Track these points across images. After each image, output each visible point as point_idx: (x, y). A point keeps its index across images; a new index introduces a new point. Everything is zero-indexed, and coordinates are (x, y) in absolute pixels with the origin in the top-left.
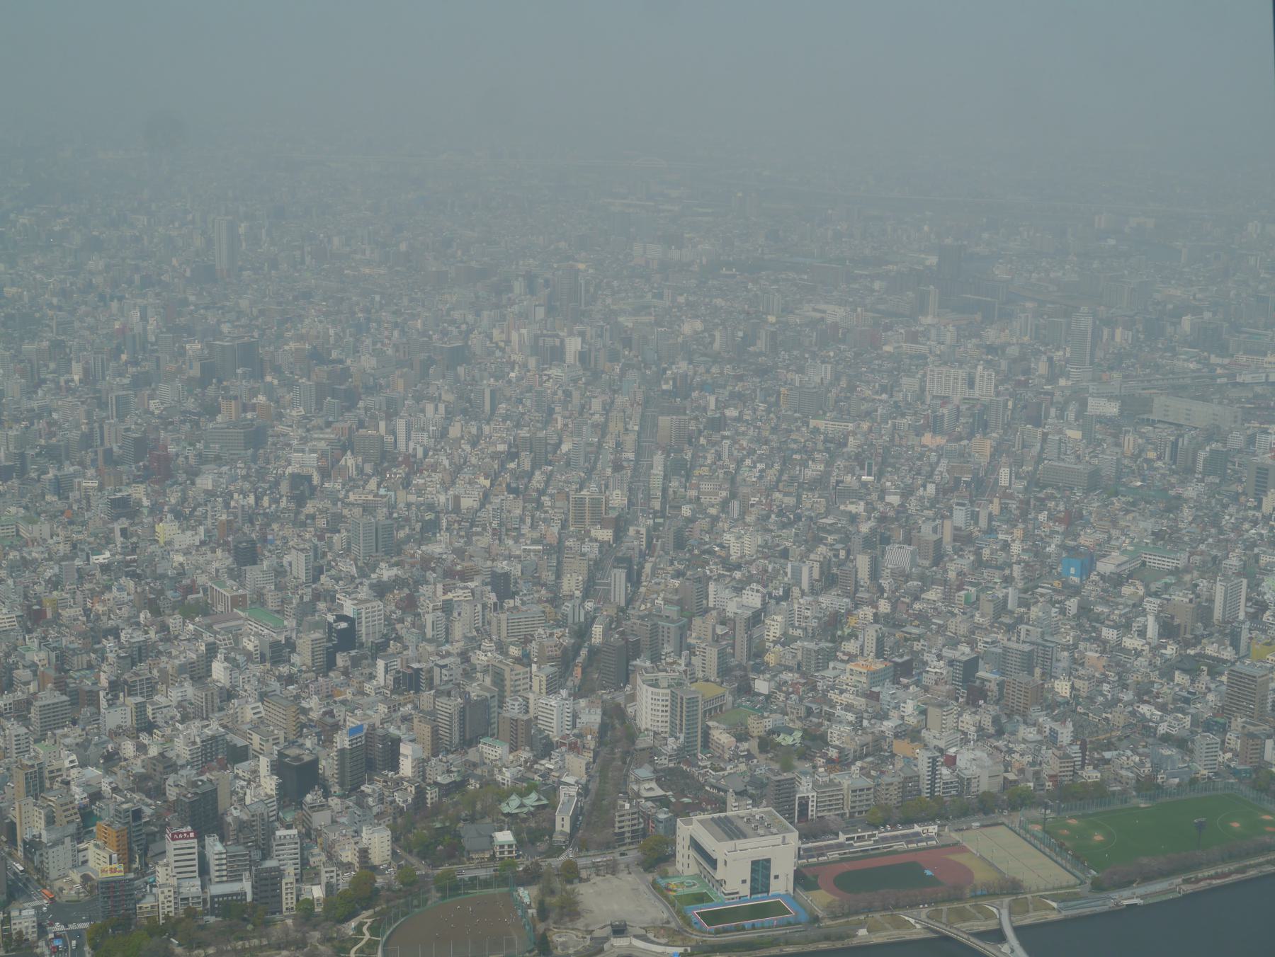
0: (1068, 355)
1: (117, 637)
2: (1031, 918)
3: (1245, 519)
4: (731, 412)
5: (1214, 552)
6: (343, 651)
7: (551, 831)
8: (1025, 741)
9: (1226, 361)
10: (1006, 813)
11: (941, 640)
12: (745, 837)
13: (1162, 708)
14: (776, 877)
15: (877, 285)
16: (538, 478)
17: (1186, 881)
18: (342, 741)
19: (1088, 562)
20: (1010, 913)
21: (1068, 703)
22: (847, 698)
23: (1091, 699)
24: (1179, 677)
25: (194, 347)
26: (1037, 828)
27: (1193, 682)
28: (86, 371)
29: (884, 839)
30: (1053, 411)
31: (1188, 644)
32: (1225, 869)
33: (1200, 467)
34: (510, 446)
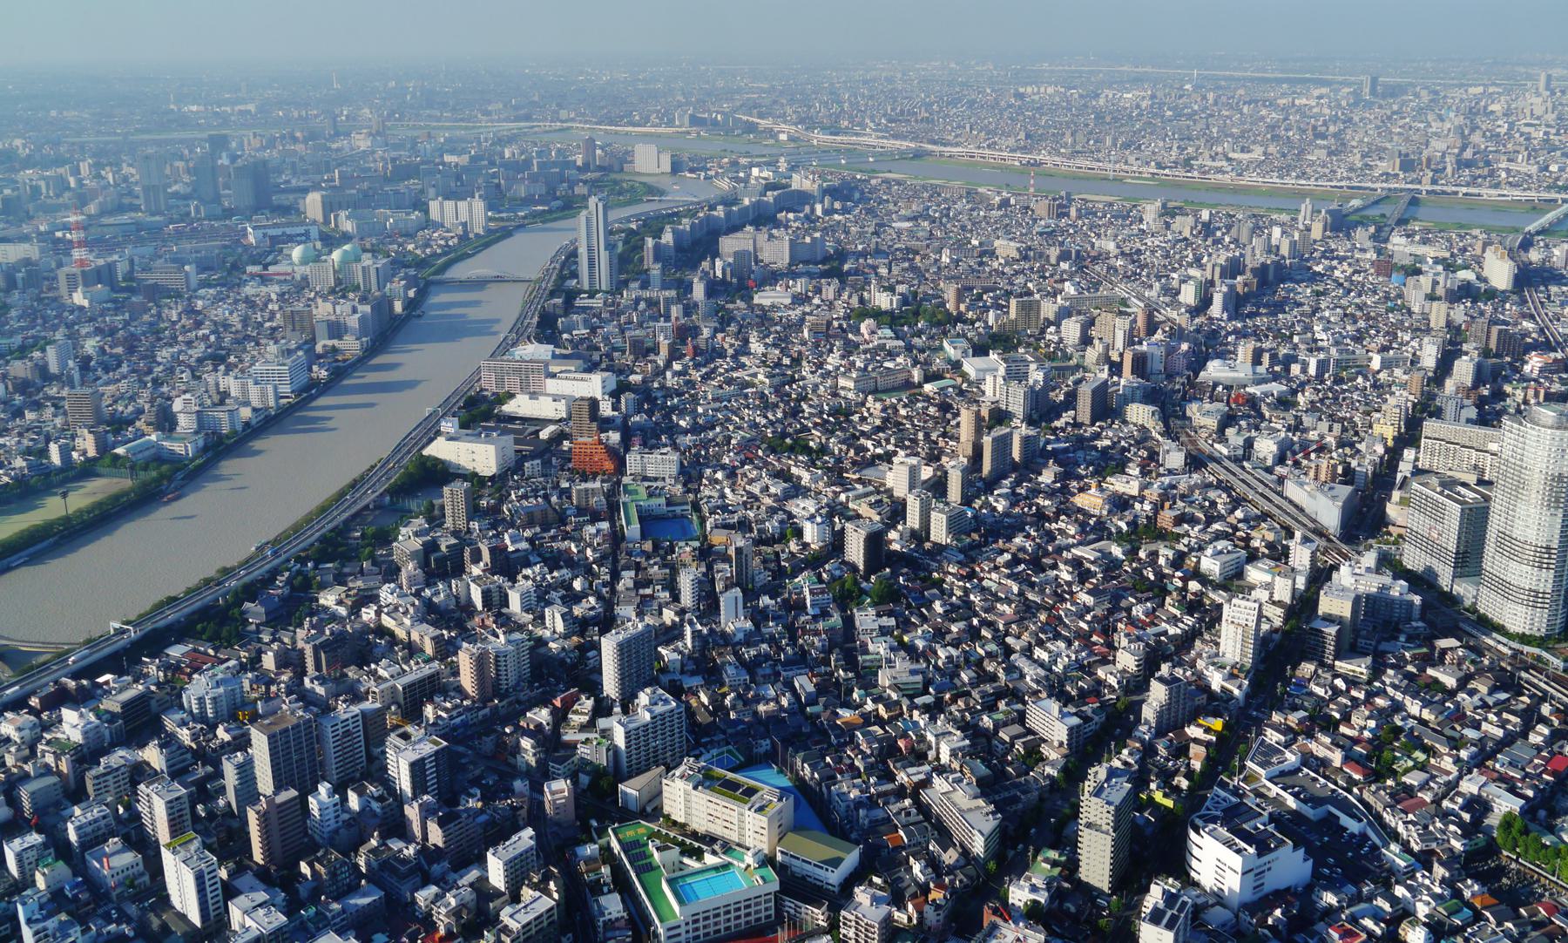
24: (30, 416)
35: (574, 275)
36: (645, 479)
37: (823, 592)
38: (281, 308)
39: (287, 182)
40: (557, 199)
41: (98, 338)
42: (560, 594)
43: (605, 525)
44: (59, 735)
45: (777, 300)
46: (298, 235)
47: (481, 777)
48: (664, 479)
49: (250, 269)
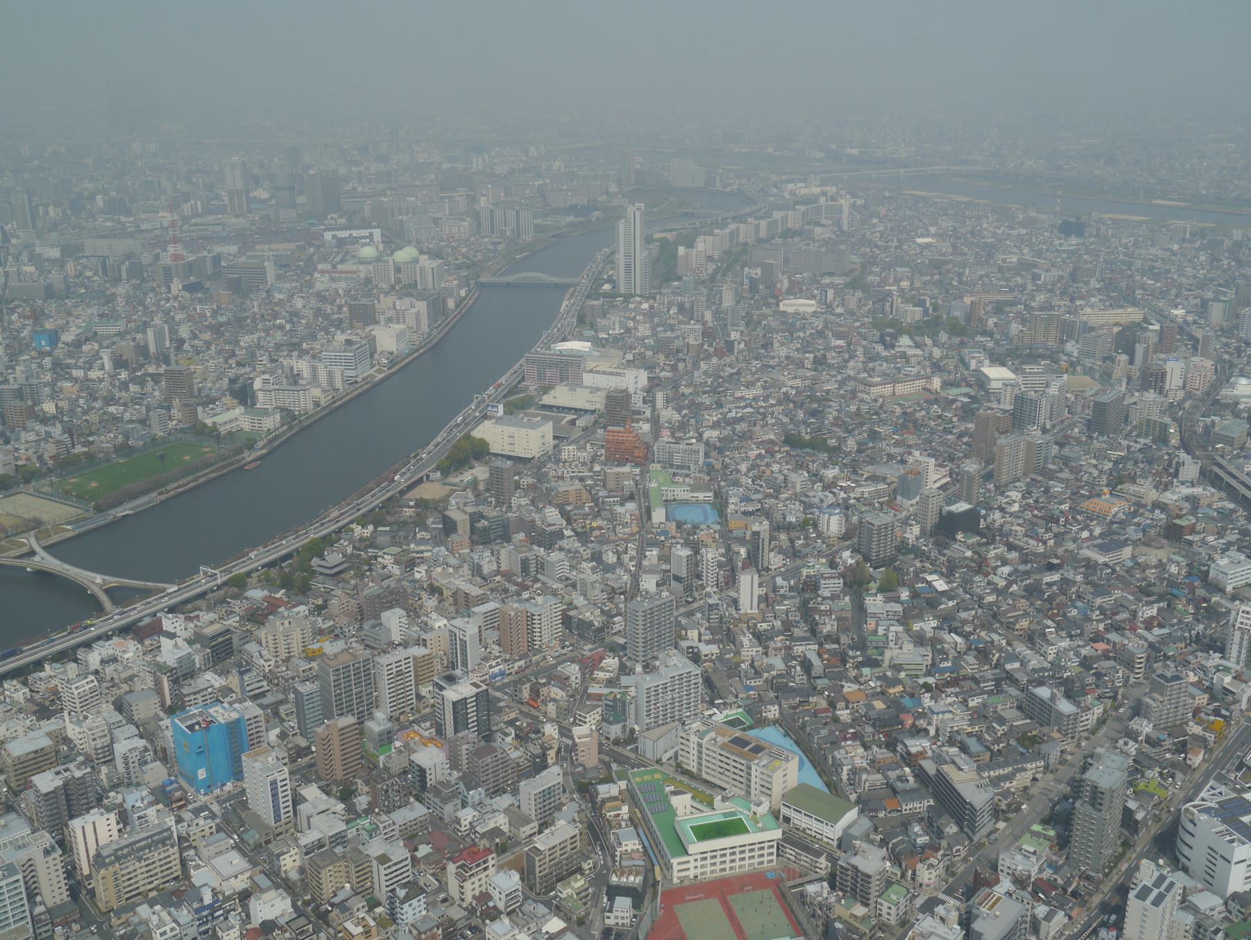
0: (15, 227)
2: (55, 539)
3: (161, 299)
5: (144, 319)
8: (27, 442)
9: (132, 219)
10: (22, 486)
13: (125, 405)
17: (160, 494)
19: (54, 338)
20: (37, 539)
21: (56, 417)
23: (72, 411)
24: (133, 388)
26: (47, 489)
27: (143, 389)
30: (10, 258)
31: (135, 370)
32: (185, 481)
33: (124, 276)
35: (610, 280)
36: (671, 466)
37: (834, 578)
38: (346, 303)
39: (354, 189)
40: (597, 209)
41: (190, 324)
42: (590, 565)
43: (631, 506)
44: (158, 659)
45: (802, 309)
46: (363, 237)
47: (516, 719)
48: (689, 468)
49: (320, 267)
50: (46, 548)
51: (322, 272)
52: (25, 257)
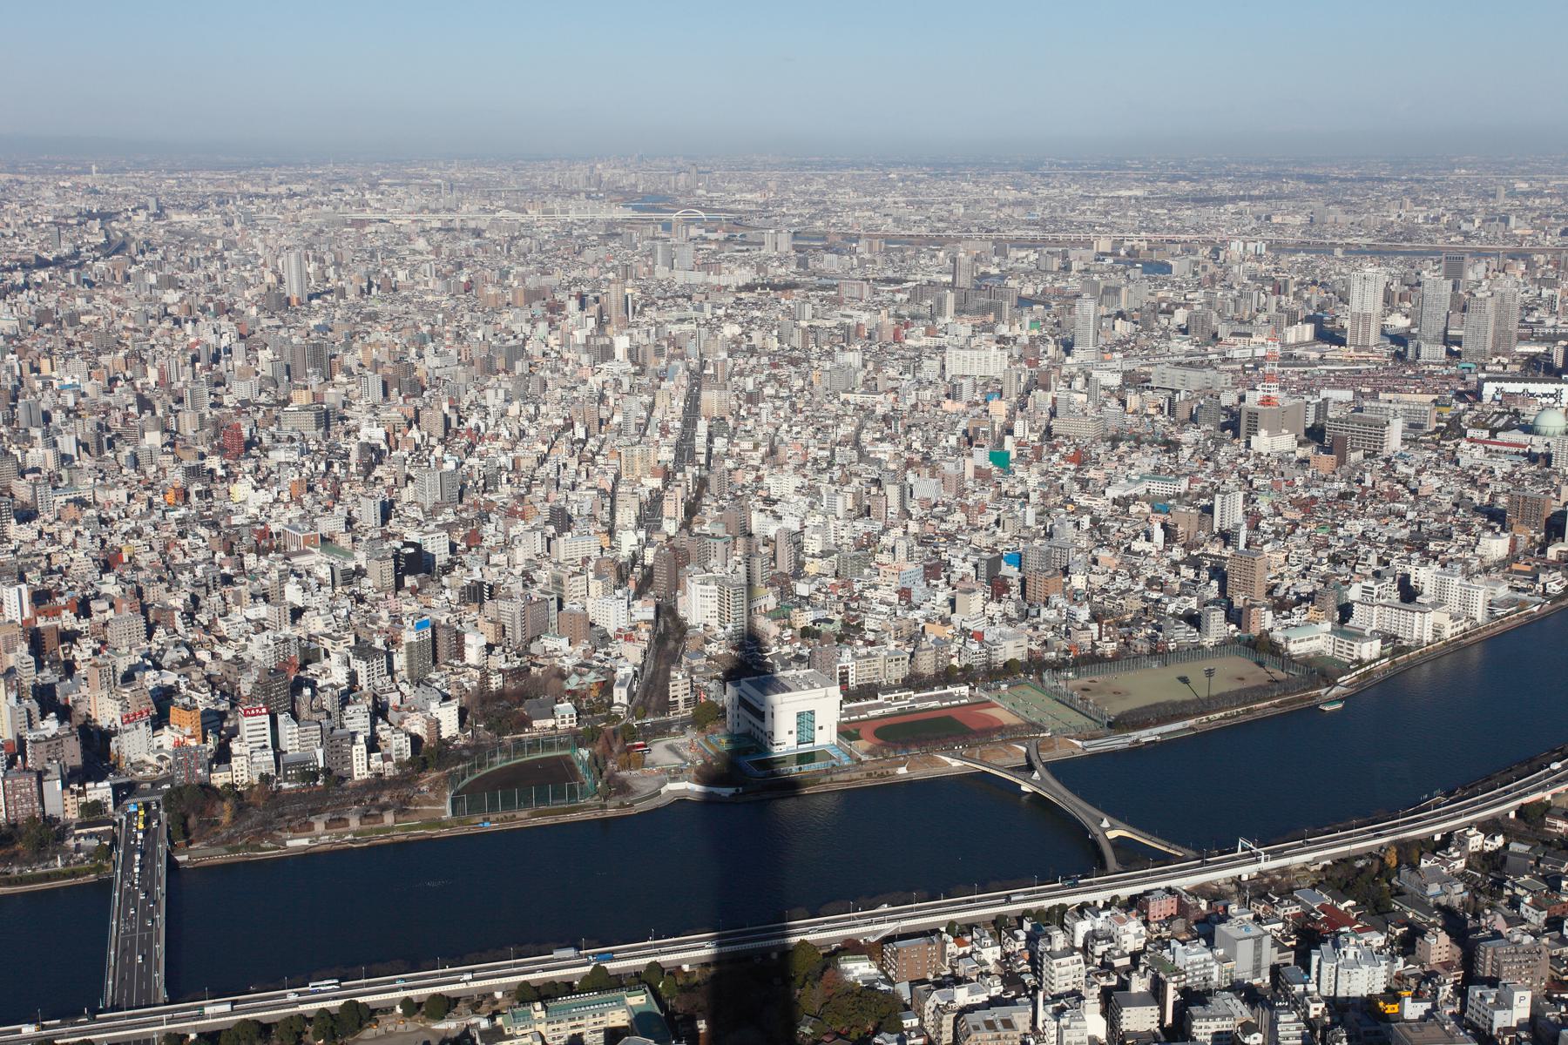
1: (192, 572)
2: (1059, 753)
4: (768, 391)
5: (1213, 479)
6: (410, 574)
7: (611, 704)
11: (967, 550)
12: (789, 690)
14: (821, 728)
15: (899, 297)
16: (592, 444)
18: (409, 636)
22: (882, 593)
24: (1184, 570)
25: (265, 355)
28: (162, 374)
29: (921, 700)
34: (565, 419)
39: (1540, 322)
49: (1470, 433)
50: (1046, 765)
51: (1472, 440)
52: (1078, 383)
